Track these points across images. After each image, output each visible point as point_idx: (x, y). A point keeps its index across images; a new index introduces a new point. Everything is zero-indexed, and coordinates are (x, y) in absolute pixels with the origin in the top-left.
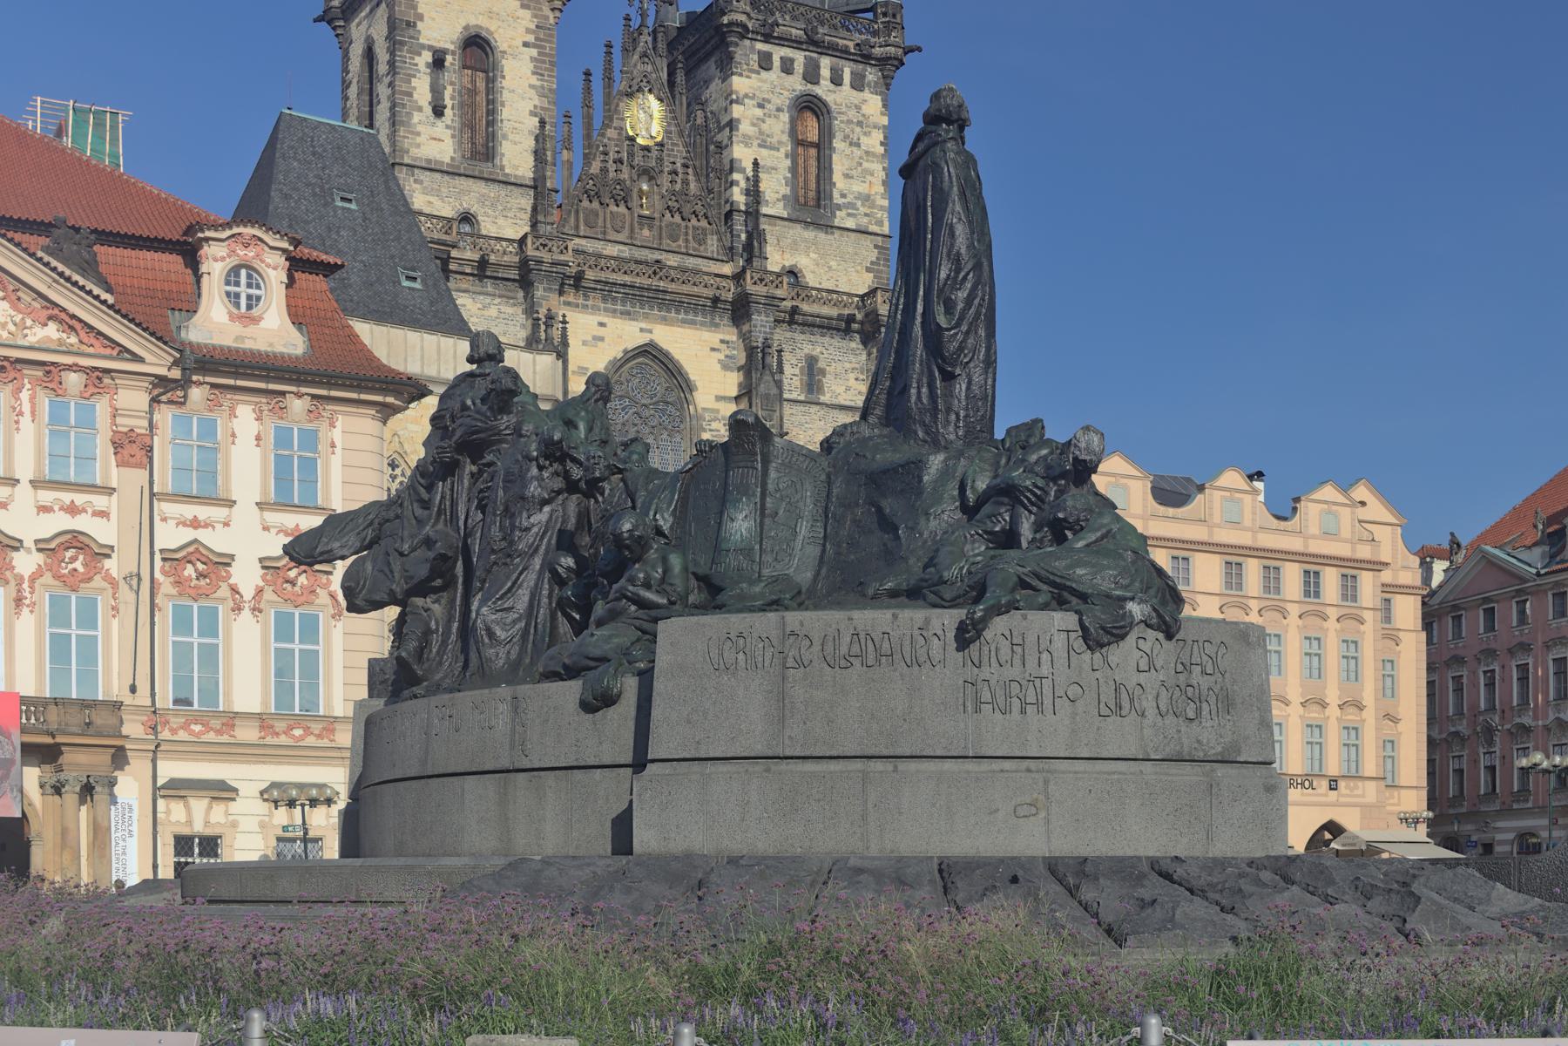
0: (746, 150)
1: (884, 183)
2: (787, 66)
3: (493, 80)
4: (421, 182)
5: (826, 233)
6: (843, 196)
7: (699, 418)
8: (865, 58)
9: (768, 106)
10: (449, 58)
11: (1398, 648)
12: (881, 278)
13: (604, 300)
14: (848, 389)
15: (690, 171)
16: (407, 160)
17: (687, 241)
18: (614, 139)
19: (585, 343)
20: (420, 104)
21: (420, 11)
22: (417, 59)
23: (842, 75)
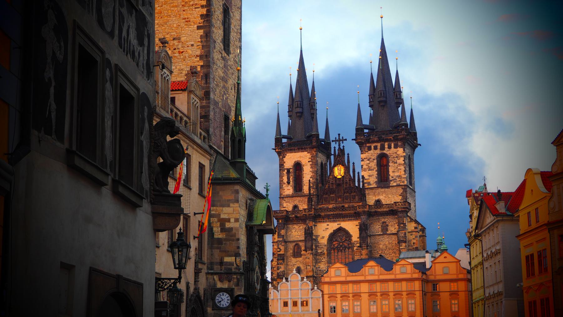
0: (365, 172)
1: (405, 171)
2: (376, 148)
3: (301, 172)
4: (285, 200)
5: (388, 188)
6: (392, 177)
8: (396, 139)
9: (370, 159)
10: (291, 170)
11: (458, 297)
12: (404, 197)
13: (328, 219)
14: (395, 228)
16: (282, 196)
17: (350, 199)
18: (331, 178)
19: (324, 230)
21: (284, 161)
22: (284, 172)
23: (391, 146)
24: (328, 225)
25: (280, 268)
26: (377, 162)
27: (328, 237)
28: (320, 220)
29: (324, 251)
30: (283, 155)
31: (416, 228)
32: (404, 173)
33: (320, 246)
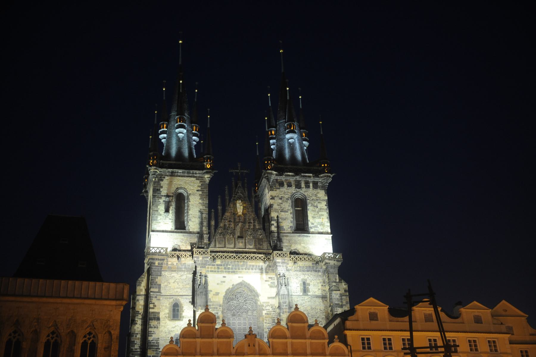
2: (289, 185)
6: (312, 224)
7: (263, 306)
13: (225, 268)
14: (319, 289)
15: (256, 222)
19: (218, 284)
20: (161, 213)
21: (161, 185)
24: (224, 277)
25: (153, 333)
26: (292, 202)
27: (225, 293)
28: (213, 270)
29: (218, 314)
30: (160, 177)
31: (345, 291)
32: (327, 221)
33: (213, 305)
